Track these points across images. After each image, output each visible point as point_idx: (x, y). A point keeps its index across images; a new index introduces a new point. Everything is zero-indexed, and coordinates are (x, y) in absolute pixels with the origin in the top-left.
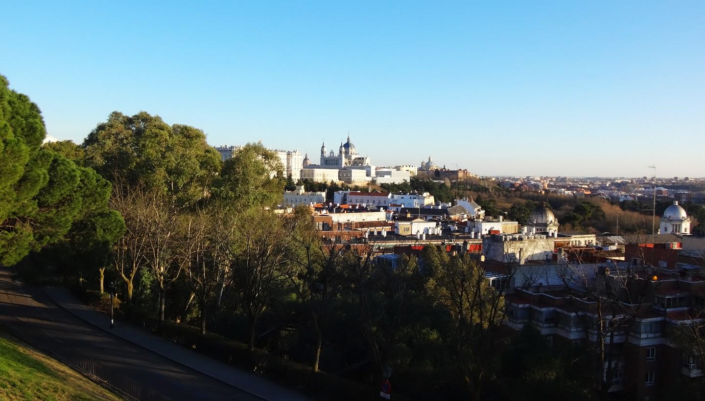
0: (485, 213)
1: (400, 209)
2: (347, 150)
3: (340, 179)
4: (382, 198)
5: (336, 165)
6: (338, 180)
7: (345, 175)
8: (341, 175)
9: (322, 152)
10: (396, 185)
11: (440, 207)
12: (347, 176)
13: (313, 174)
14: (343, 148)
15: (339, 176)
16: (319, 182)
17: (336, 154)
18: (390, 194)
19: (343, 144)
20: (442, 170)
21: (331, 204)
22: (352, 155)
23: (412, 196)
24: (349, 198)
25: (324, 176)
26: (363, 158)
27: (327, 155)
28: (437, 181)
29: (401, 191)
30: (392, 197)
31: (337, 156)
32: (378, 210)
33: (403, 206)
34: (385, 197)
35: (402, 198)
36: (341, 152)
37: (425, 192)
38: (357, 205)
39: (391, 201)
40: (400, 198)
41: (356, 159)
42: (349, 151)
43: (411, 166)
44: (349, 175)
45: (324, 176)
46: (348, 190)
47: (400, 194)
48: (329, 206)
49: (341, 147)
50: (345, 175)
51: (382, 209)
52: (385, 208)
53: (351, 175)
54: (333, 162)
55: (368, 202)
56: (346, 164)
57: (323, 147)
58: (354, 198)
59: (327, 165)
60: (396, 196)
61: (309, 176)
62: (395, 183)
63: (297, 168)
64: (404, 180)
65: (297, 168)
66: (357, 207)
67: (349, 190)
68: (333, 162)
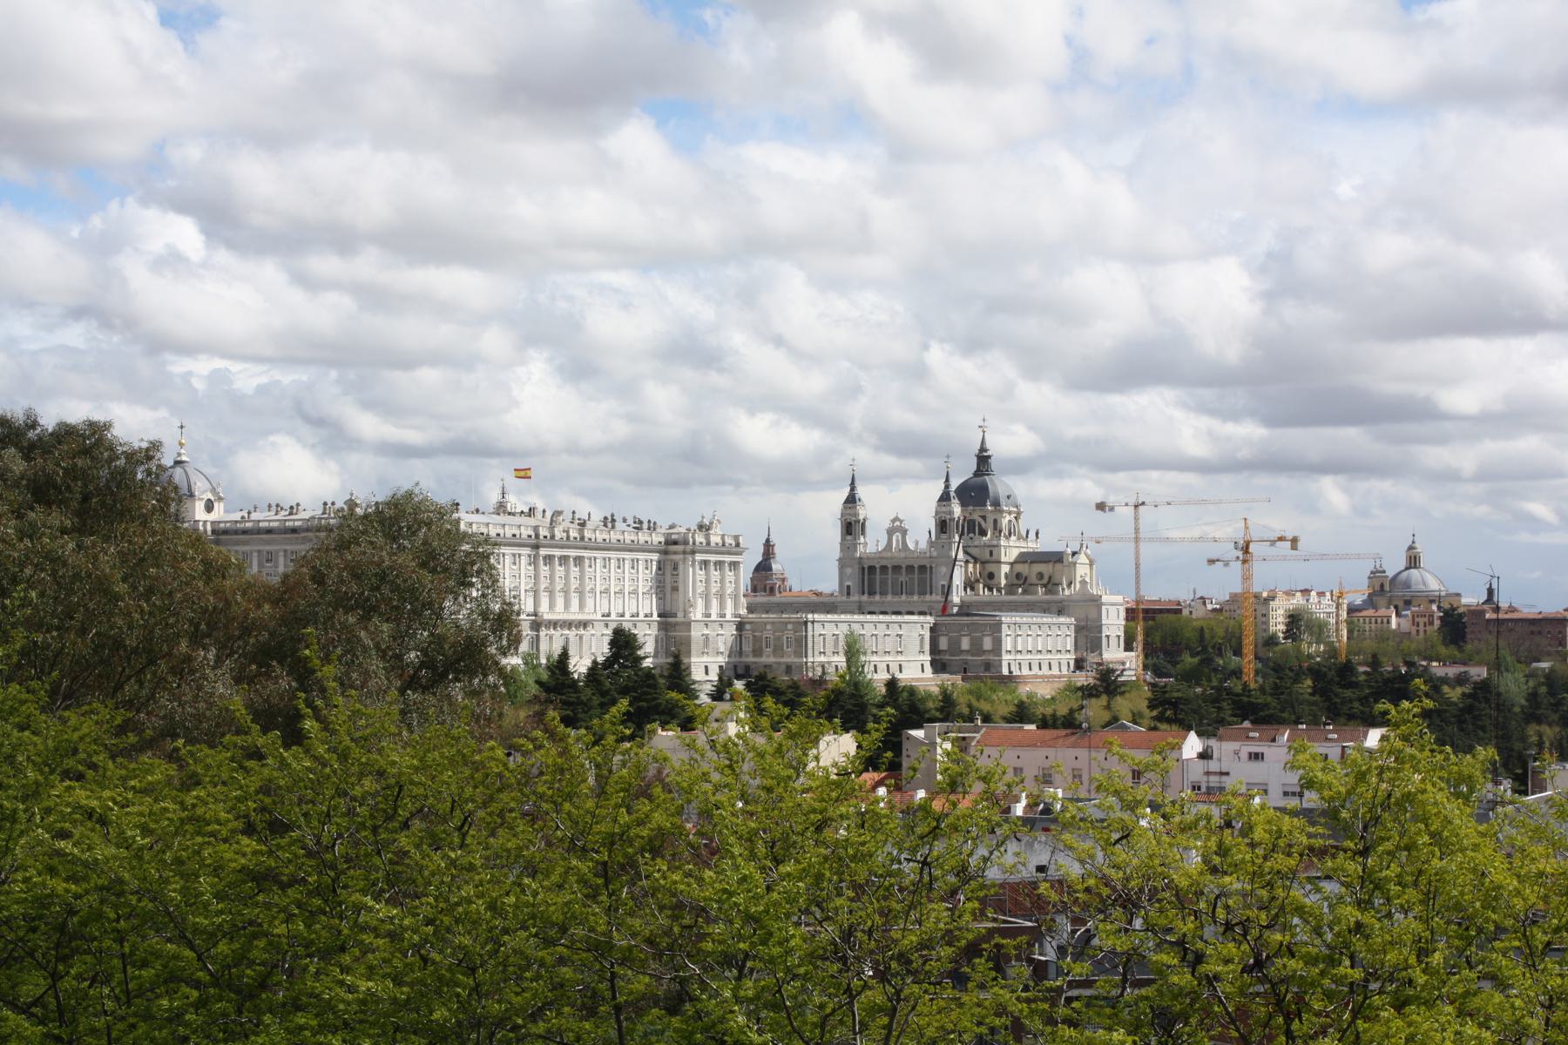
2: (976, 517)
3: (939, 666)
5: (922, 593)
7: (965, 644)
8: (943, 643)
9: (851, 528)
12: (977, 648)
13: (801, 645)
14: (957, 510)
15: (934, 650)
16: (832, 677)
17: (920, 534)
19: (954, 484)
20: (1477, 613)
22: (1003, 542)
25: (853, 651)
26: (1056, 558)
27: (872, 543)
29: (1247, 724)
30: (1204, 755)
31: (923, 545)
35: (1256, 757)
36: (943, 526)
39: (1197, 772)
41: (1024, 558)
42: (984, 518)
43: (1313, 593)
44: (987, 644)
45: (853, 651)
49: (945, 498)
50: (965, 644)
53: (998, 643)
54: (903, 578)
56: (970, 585)
57: (851, 500)
59: (872, 593)
60: (1225, 750)
66: (1019, 810)
68: (903, 578)
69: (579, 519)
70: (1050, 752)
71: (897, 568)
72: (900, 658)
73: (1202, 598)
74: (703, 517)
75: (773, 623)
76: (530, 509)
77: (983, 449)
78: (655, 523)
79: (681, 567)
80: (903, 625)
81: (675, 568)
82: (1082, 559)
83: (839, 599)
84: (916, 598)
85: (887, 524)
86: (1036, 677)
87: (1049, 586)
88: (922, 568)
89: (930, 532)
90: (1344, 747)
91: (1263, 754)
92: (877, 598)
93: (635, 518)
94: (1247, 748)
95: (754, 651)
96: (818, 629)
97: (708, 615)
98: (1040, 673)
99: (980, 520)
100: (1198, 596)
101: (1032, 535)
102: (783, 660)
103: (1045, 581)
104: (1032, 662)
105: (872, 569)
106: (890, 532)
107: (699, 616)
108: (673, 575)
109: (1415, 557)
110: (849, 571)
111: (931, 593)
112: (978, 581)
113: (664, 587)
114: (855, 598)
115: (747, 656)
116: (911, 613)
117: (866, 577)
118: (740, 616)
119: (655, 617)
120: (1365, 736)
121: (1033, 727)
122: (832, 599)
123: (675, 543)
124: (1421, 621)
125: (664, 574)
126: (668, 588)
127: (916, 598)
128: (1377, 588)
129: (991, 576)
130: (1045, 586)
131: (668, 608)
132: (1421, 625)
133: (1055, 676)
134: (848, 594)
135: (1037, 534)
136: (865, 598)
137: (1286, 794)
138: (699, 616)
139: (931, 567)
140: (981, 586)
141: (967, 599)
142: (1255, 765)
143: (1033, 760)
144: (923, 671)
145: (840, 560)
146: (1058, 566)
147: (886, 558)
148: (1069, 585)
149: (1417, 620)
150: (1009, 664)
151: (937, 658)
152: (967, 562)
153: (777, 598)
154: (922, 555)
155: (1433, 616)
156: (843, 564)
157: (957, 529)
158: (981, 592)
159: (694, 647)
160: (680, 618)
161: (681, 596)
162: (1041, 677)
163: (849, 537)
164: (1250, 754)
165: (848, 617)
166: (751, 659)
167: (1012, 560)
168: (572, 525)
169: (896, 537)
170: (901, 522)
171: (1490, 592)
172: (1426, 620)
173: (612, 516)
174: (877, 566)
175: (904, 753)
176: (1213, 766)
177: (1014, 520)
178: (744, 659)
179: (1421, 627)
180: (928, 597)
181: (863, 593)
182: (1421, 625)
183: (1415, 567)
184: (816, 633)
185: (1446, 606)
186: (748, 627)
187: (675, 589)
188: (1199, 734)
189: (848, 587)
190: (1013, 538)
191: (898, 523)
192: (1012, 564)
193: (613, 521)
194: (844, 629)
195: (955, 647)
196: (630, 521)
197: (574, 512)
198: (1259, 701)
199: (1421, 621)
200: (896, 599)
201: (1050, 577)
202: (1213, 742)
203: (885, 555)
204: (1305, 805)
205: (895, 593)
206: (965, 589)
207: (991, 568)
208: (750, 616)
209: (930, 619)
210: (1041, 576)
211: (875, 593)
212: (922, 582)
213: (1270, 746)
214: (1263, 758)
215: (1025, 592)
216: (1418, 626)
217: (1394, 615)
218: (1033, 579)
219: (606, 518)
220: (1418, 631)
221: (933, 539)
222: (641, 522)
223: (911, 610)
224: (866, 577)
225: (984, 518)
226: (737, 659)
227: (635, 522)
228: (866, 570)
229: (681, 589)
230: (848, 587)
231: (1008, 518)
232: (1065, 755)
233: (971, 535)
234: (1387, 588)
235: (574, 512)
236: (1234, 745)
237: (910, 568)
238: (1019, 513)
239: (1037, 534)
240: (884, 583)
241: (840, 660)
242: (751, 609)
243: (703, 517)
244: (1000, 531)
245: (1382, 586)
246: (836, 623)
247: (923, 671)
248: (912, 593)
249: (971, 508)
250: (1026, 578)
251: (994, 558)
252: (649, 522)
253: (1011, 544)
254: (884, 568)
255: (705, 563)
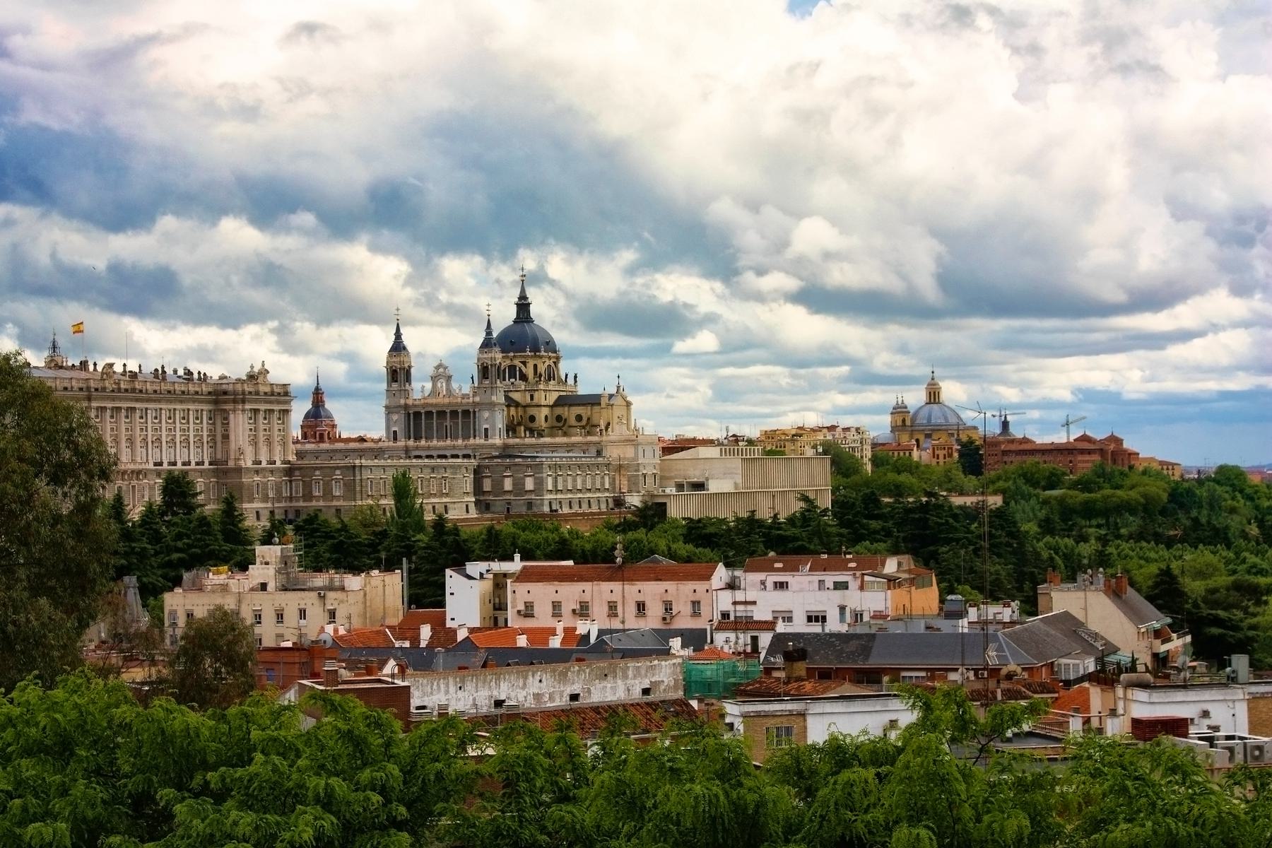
0: (1193, 643)
1: (765, 639)
2: (517, 362)
3: (483, 506)
4: (682, 592)
5: (466, 437)
6: (473, 513)
7: (508, 484)
8: (487, 485)
10: (760, 523)
11: (963, 625)
12: (519, 488)
14: (497, 356)
15: (478, 489)
18: (721, 574)
19: (495, 335)
21: (426, 632)
23: (830, 578)
24: (517, 595)
25: (402, 490)
27: (420, 388)
28: (969, 501)
30: (732, 586)
31: (467, 389)
32: (666, 653)
33: (781, 628)
34: (701, 586)
35: (781, 586)
36: (484, 371)
37: (895, 551)
38: (553, 632)
40: (770, 584)
41: (562, 402)
42: (524, 363)
44: (529, 484)
45: (402, 490)
46: (512, 559)
47: (769, 568)
48: (415, 640)
49: (487, 344)
50: (508, 484)
51: (676, 643)
52: (695, 639)
53: (540, 483)
55: (612, 609)
56: (511, 428)
58: (542, 594)
59: (417, 438)
60: (750, 579)
61: (327, 494)
62: (757, 517)
63: (264, 459)
64: (805, 499)
65: (264, 459)
67: (517, 557)
69: (131, 372)
70: (587, 586)
71: (441, 414)
72: (445, 500)
73: (734, 436)
74: (252, 367)
75: (321, 468)
76: (81, 363)
77: (523, 297)
78: (205, 374)
79: (232, 416)
80: (373, 468)
81: (226, 419)
82: (618, 401)
83: (386, 444)
84: (460, 442)
85: (430, 370)
86: (576, 514)
87: (588, 428)
88: (466, 413)
89: (472, 378)
90: (863, 574)
91: (787, 583)
92: (423, 442)
93: (185, 369)
94: (772, 578)
95: (304, 496)
96: (367, 474)
97: (260, 463)
98: (580, 511)
99: (521, 365)
100: (730, 434)
101: (571, 381)
102: (335, 503)
103: (584, 422)
104: (573, 501)
105: (417, 414)
106: (434, 379)
107: (249, 464)
108: (223, 424)
109: (935, 393)
110: (395, 417)
111: (475, 437)
112: (519, 424)
113: (215, 436)
114: (401, 443)
115: (298, 501)
116: (456, 456)
117: (412, 423)
118: (289, 462)
119: (206, 465)
120: (883, 565)
121: (571, 563)
122: (381, 444)
123: (225, 393)
124: (941, 453)
125: (214, 424)
126: (219, 438)
127: (460, 442)
128: (899, 423)
129: (532, 419)
130: (583, 427)
131: (219, 456)
132: (941, 457)
133: (593, 514)
134: (395, 439)
135: (576, 377)
136: (411, 443)
137: (810, 619)
138: (249, 464)
139: (474, 412)
140: (522, 428)
141: (512, 441)
142: (780, 594)
143: (571, 593)
144: (467, 512)
145: (387, 407)
146: (596, 408)
147: (432, 405)
148: (607, 429)
149: (937, 452)
150: (550, 503)
151: (482, 498)
152: (508, 406)
153: (325, 446)
154: (465, 401)
155: (952, 448)
156: (389, 410)
157: (499, 375)
158: (523, 435)
159: (245, 493)
160: (231, 464)
161: (233, 446)
162: (583, 514)
163: (395, 385)
164: (775, 583)
165: (395, 462)
166: (301, 504)
167: (551, 403)
168: (123, 378)
169: (442, 385)
170: (446, 368)
171: (1005, 425)
172: (945, 452)
173: (163, 367)
174: (423, 411)
175: (448, 591)
176: (740, 596)
177: (553, 365)
178: (295, 504)
179: (941, 460)
180: (472, 441)
181: (409, 438)
182: (941, 457)
183: (935, 403)
184: (364, 477)
185: (964, 438)
186: (297, 473)
187: (226, 437)
188: (727, 565)
189: (395, 432)
190: (552, 382)
191: (441, 370)
192: (551, 407)
193: (164, 372)
194: (389, 475)
195: (498, 489)
196: (181, 372)
197: (125, 365)
198: (788, 533)
199: (941, 453)
200: (441, 443)
201: (589, 419)
202: (738, 573)
203: (430, 401)
204: (827, 631)
205: (439, 439)
206: (508, 433)
207: (532, 411)
208: (299, 462)
209: (474, 462)
210: (579, 418)
211: (421, 438)
212: (466, 426)
213: (794, 576)
214: (787, 587)
215: (565, 434)
216: (938, 458)
217: (915, 448)
218: (573, 421)
219: (156, 370)
220: (938, 463)
221: (476, 385)
222: (192, 374)
223: (455, 452)
224: (412, 423)
225: (524, 363)
226: (288, 504)
227: (185, 374)
228: (412, 415)
229: (232, 437)
230: (395, 432)
231: (546, 364)
232: (601, 592)
233: (512, 380)
234: (908, 423)
235: (125, 365)
236: (761, 576)
237: (454, 414)
238: (558, 358)
239: (576, 377)
240: (429, 427)
241: (388, 502)
242: (300, 455)
243: (252, 367)
244: (541, 375)
245: (904, 421)
246: (384, 467)
247: (467, 512)
248: (457, 438)
249: (512, 354)
250: (566, 420)
251: (535, 401)
252: (199, 373)
253: (551, 388)
254: (429, 414)
255: (256, 411)
